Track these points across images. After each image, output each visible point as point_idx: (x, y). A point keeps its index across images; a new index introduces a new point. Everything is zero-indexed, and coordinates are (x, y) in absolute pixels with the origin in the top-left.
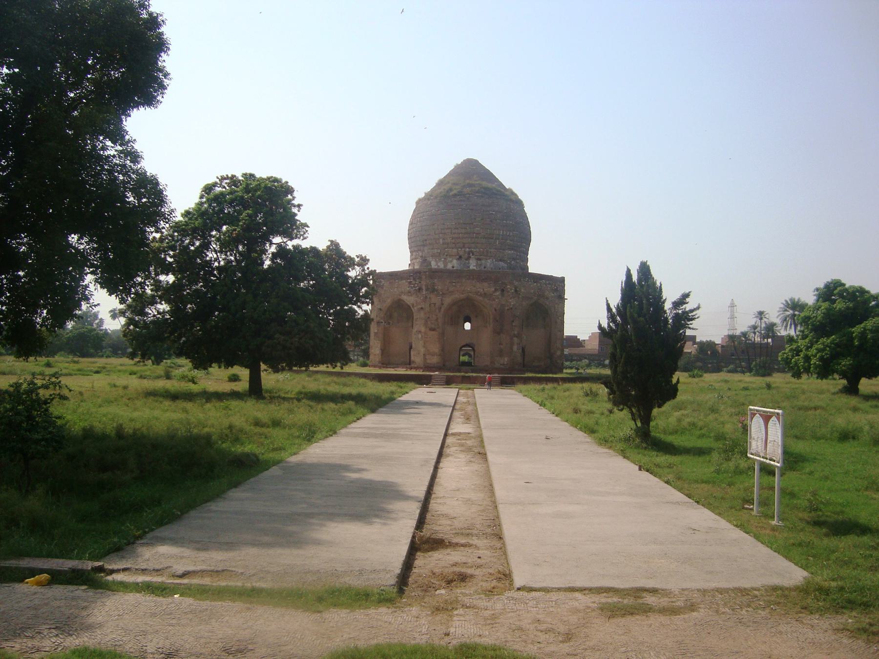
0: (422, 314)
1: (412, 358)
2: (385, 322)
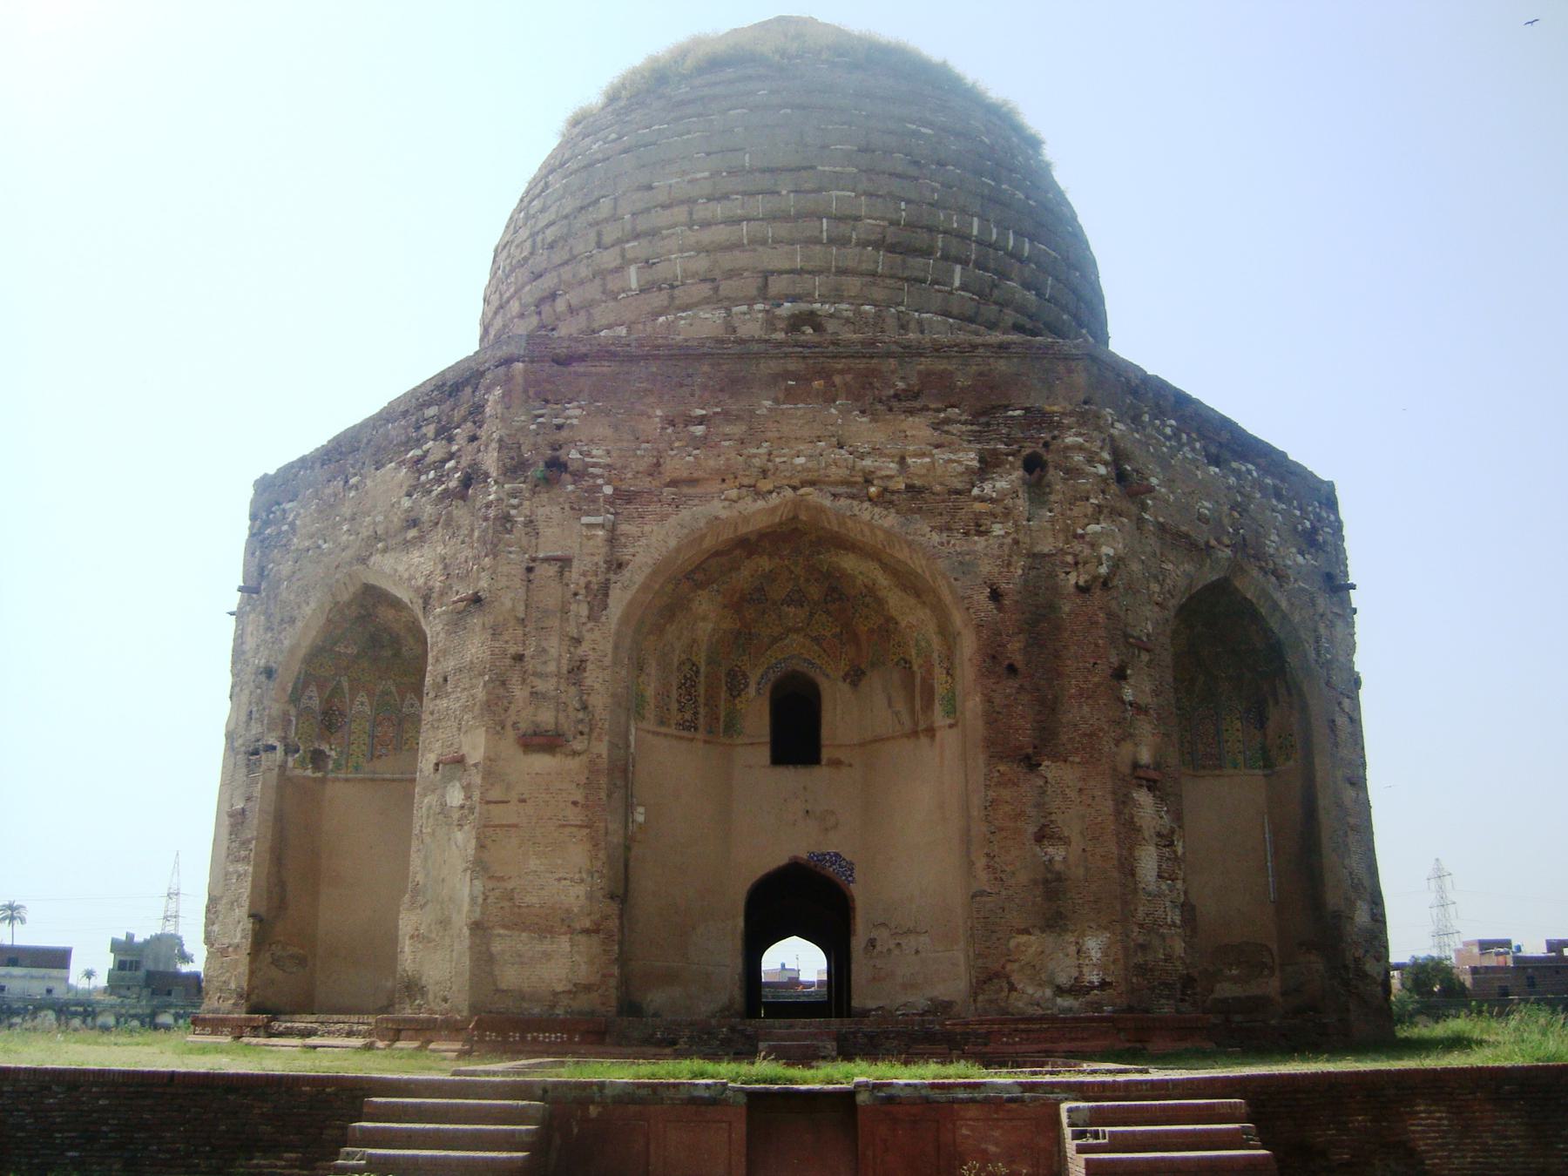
0: (476, 647)
1: (409, 957)
2: (290, 749)
